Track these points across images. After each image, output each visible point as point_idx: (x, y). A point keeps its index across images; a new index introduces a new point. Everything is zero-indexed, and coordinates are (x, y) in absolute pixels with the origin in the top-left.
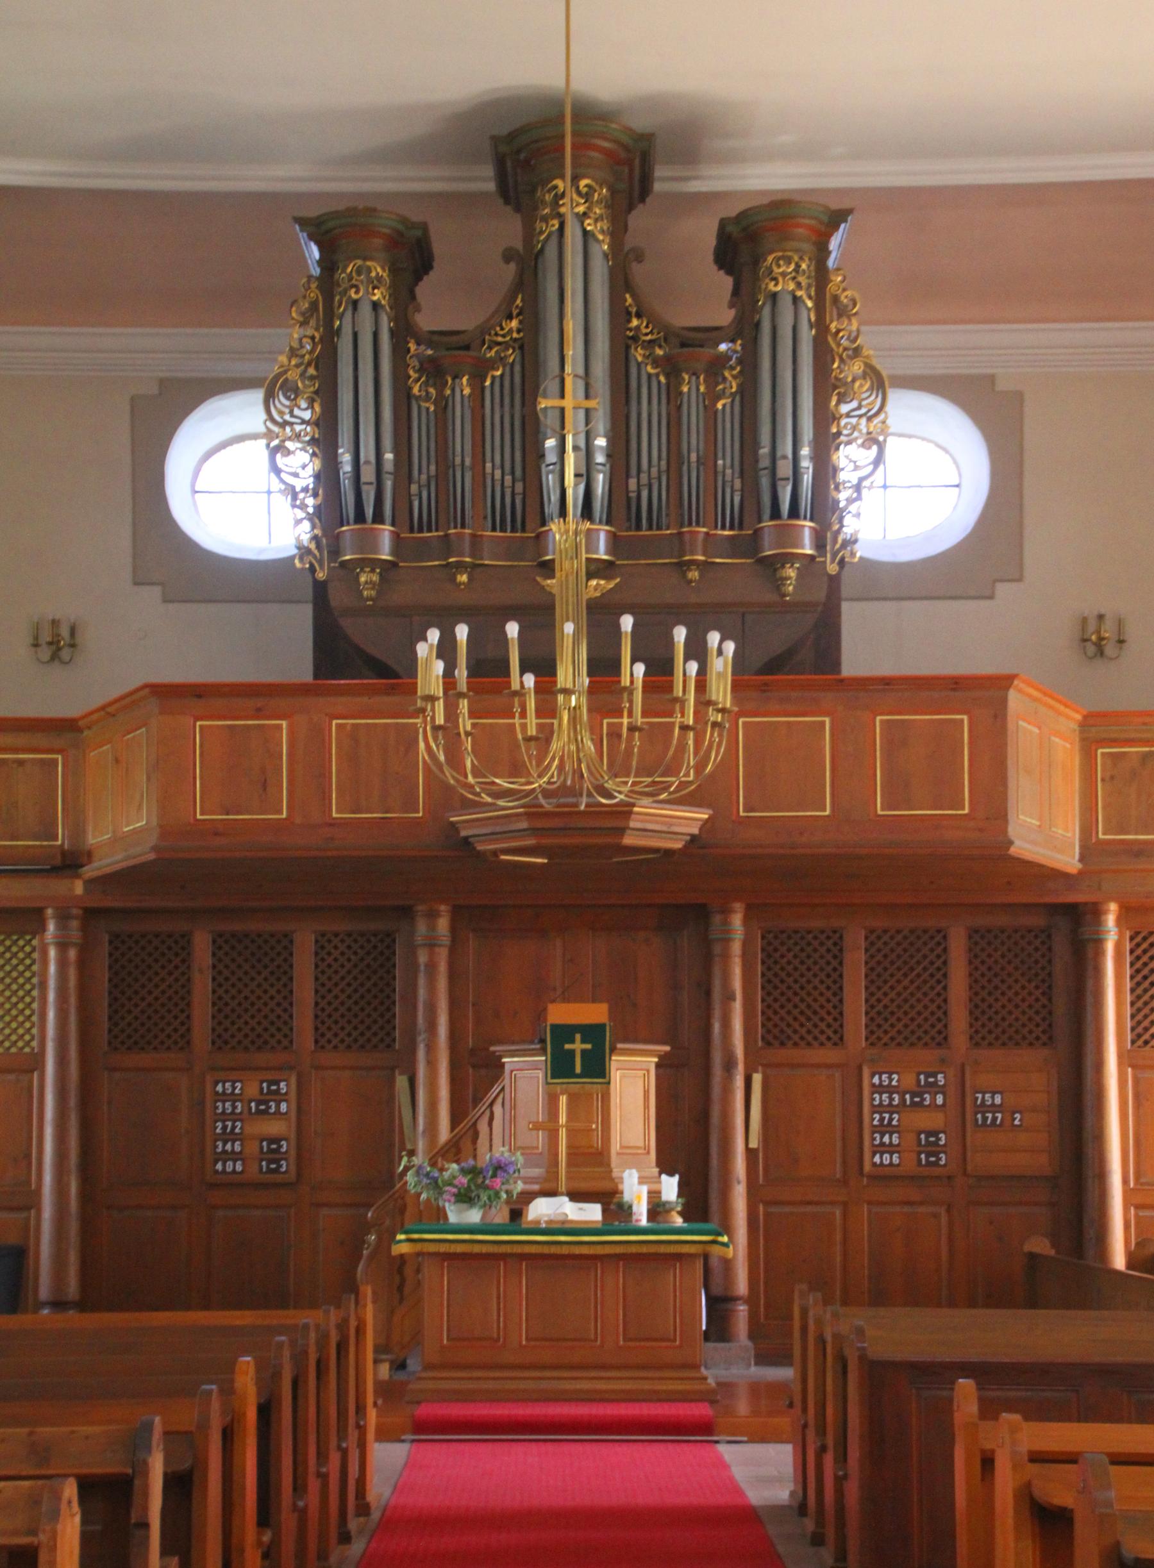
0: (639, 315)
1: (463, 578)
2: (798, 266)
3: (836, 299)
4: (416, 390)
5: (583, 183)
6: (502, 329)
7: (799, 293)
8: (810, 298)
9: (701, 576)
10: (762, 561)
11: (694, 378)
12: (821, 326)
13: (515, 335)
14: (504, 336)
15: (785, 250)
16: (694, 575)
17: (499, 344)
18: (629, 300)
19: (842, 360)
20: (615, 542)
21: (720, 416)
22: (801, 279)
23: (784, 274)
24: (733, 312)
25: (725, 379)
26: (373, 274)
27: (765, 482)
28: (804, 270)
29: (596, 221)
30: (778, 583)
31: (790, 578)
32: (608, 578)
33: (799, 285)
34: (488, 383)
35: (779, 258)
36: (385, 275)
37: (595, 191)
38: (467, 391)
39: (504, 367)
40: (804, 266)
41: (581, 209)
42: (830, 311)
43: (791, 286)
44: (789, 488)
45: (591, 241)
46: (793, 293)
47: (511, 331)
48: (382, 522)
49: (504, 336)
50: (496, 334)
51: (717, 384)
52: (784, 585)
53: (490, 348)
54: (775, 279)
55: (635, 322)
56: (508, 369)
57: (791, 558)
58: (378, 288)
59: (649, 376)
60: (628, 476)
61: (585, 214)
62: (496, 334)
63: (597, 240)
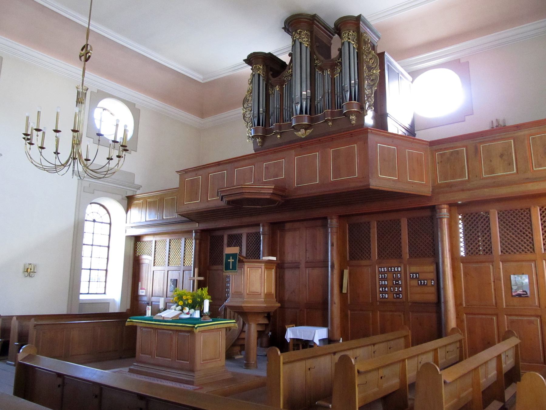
0: (317, 60)
1: (279, 136)
2: (348, 34)
3: (364, 40)
4: (270, 93)
5: (298, 31)
6: (288, 72)
7: (349, 41)
8: (354, 41)
9: (332, 124)
10: (345, 114)
11: (326, 71)
12: (359, 48)
13: (291, 73)
14: (288, 74)
15: (345, 31)
16: (330, 124)
17: (286, 76)
18: (315, 57)
19: (366, 56)
20: (312, 120)
21: (336, 79)
22: (349, 37)
23: (345, 37)
24: (339, 52)
25: (337, 69)
26: (258, 67)
27: (343, 92)
28: (350, 35)
29: (302, 39)
30: (350, 121)
31: (353, 119)
32: (312, 129)
33: (349, 39)
34: (284, 86)
35: (344, 33)
36: (261, 67)
37: (302, 32)
38: (278, 89)
39: (288, 82)
40: (350, 33)
41: (298, 37)
42: (362, 43)
43: (347, 39)
44: (349, 93)
45: (302, 44)
46: (347, 41)
47: (290, 72)
48: (260, 126)
49: (288, 74)
50: (286, 74)
51: (335, 71)
52: (351, 121)
53: (285, 78)
54: (343, 39)
55: (316, 61)
56: (289, 82)
57: (350, 113)
58: (259, 70)
59: (320, 74)
60: (315, 101)
61: (299, 38)
62: (286, 74)
63: (304, 44)
